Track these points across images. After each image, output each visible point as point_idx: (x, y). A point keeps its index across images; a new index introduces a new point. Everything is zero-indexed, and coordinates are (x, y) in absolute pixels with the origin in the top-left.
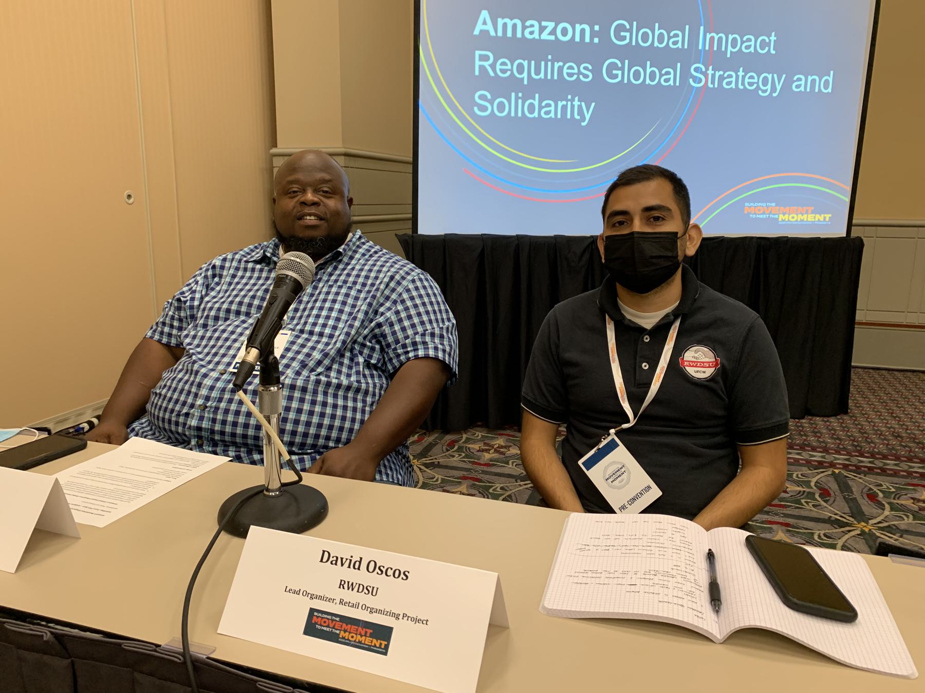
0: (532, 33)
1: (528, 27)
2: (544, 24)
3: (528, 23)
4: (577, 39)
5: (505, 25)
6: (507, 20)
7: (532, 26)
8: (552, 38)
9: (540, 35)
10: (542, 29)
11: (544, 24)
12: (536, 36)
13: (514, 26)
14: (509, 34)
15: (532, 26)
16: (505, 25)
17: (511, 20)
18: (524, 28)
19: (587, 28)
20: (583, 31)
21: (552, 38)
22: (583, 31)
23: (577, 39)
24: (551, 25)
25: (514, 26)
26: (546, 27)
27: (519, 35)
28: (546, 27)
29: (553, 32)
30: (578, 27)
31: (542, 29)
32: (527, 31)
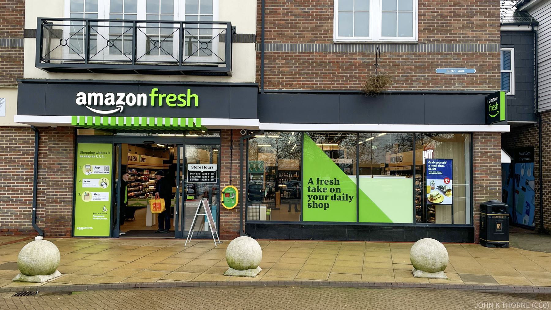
0: (109, 101)
2: (118, 94)
3: (107, 95)
4: (139, 104)
5: (93, 97)
6: (94, 94)
7: (110, 97)
8: (124, 103)
9: (116, 100)
10: (116, 98)
11: (118, 94)
12: (113, 103)
14: (95, 103)
16: (93, 97)
18: (105, 98)
19: (144, 96)
20: (142, 98)
21: (124, 103)
22: (142, 98)
23: (139, 104)
24: (122, 95)
25: (99, 97)
27: (101, 103)
28: (119, 97)
29: (124, 100)
30: (139, 96)
31: (116, 98)
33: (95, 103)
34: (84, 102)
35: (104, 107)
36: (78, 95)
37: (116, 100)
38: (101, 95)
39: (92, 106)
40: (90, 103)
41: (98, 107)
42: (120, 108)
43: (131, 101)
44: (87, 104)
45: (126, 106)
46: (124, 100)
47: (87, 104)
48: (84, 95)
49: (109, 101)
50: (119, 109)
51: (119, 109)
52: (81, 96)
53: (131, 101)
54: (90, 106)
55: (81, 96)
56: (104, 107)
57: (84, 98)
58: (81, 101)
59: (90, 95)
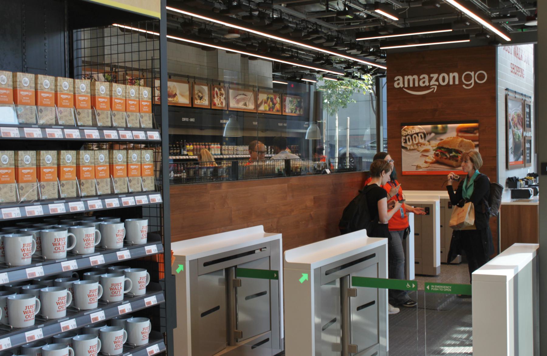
0: (424, 82)
1: (421, 79)
3: (421, 77)
4: (451, 83)
5: (409, 80)
6: (411, 77)
7: (424, 78)
8: (437, 83)
9: (429, 82)
10: (430, 79)
11: (432, 75)
12: (427, 84)
13: (414, 80)
14: (411, 85)
15: (424, 78)
16: (409, 80)
17: (412, 76)
19: (456, 74)
20: (454, 77)
21: (437, 83)
22: (454, 77)
23: (451, 83)
24: (435, 76)
25: (414, 80)
26: (433, 77)
27: (416, 85)
28: (433, 77)
29: (437, 80)
30: (451, 75)
31: (430, 79)
32: (421, 82)
33: (411, 85)
34: (401, 85)
35: (420, 89)
36: (396, 79)
37: (429, 82)
38: (416, 77)
39: (409, 88)
40: (406, 86)
41: (414, 89)
42: (434, 88)
43: (444, 80)
44: (404, 87)
45: (439, 86)
46: (437, 80)
47: (404, 87)
48: (401, 78)
49: (424, 82)
50: (433, 89)
51: (433, 89)
52: (398, 80)
53: (444, 80)
54: (406, 88)
55: (398, 80)
56: (420, 89)
57: (401, 81)
58: (398, 84)
59: (406, 78)
